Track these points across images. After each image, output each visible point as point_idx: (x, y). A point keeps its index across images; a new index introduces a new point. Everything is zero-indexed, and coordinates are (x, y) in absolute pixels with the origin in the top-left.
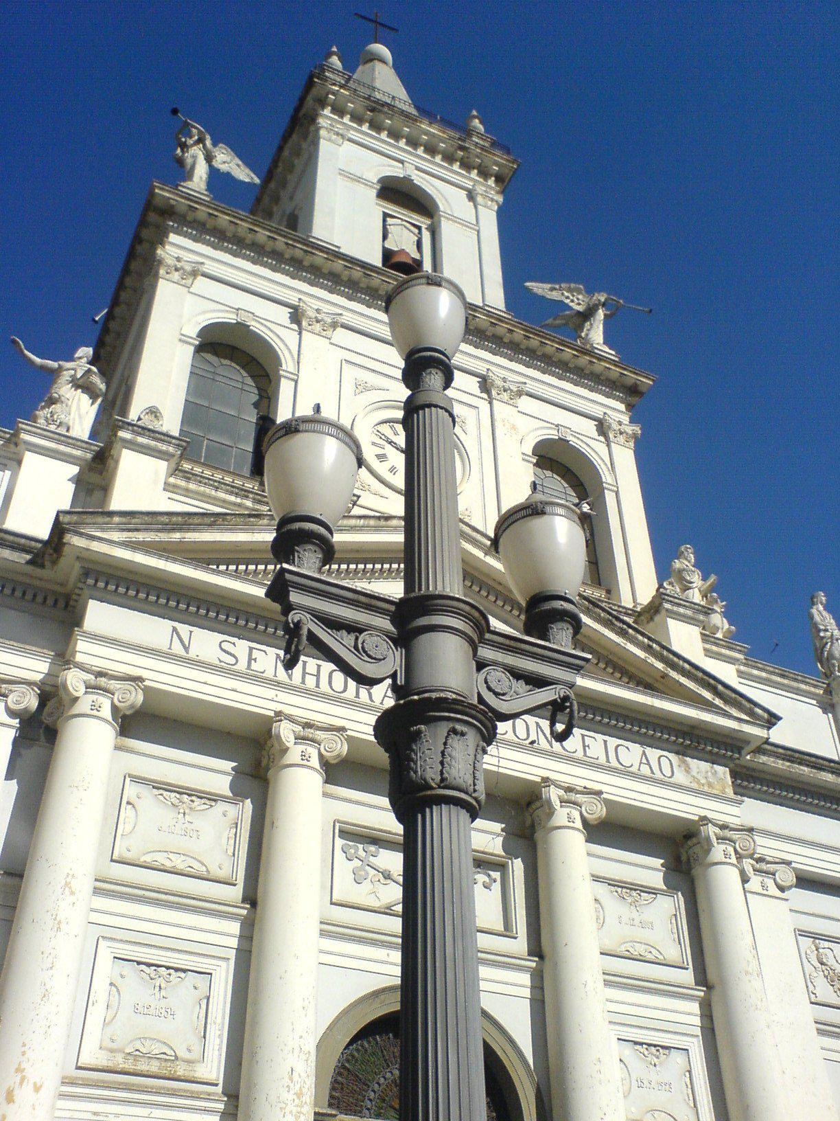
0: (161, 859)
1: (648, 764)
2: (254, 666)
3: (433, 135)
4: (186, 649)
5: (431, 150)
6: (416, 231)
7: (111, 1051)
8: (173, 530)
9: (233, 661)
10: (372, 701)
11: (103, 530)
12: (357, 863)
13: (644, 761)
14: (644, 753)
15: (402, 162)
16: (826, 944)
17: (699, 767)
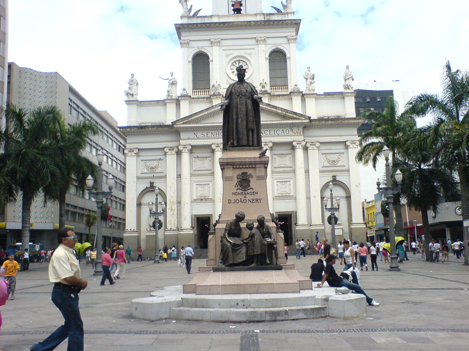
0: (200, 169)
4: (197, 136)
8: (189, 118)
11: (179, 122)
16: (328, 155)
17: (295, 130)
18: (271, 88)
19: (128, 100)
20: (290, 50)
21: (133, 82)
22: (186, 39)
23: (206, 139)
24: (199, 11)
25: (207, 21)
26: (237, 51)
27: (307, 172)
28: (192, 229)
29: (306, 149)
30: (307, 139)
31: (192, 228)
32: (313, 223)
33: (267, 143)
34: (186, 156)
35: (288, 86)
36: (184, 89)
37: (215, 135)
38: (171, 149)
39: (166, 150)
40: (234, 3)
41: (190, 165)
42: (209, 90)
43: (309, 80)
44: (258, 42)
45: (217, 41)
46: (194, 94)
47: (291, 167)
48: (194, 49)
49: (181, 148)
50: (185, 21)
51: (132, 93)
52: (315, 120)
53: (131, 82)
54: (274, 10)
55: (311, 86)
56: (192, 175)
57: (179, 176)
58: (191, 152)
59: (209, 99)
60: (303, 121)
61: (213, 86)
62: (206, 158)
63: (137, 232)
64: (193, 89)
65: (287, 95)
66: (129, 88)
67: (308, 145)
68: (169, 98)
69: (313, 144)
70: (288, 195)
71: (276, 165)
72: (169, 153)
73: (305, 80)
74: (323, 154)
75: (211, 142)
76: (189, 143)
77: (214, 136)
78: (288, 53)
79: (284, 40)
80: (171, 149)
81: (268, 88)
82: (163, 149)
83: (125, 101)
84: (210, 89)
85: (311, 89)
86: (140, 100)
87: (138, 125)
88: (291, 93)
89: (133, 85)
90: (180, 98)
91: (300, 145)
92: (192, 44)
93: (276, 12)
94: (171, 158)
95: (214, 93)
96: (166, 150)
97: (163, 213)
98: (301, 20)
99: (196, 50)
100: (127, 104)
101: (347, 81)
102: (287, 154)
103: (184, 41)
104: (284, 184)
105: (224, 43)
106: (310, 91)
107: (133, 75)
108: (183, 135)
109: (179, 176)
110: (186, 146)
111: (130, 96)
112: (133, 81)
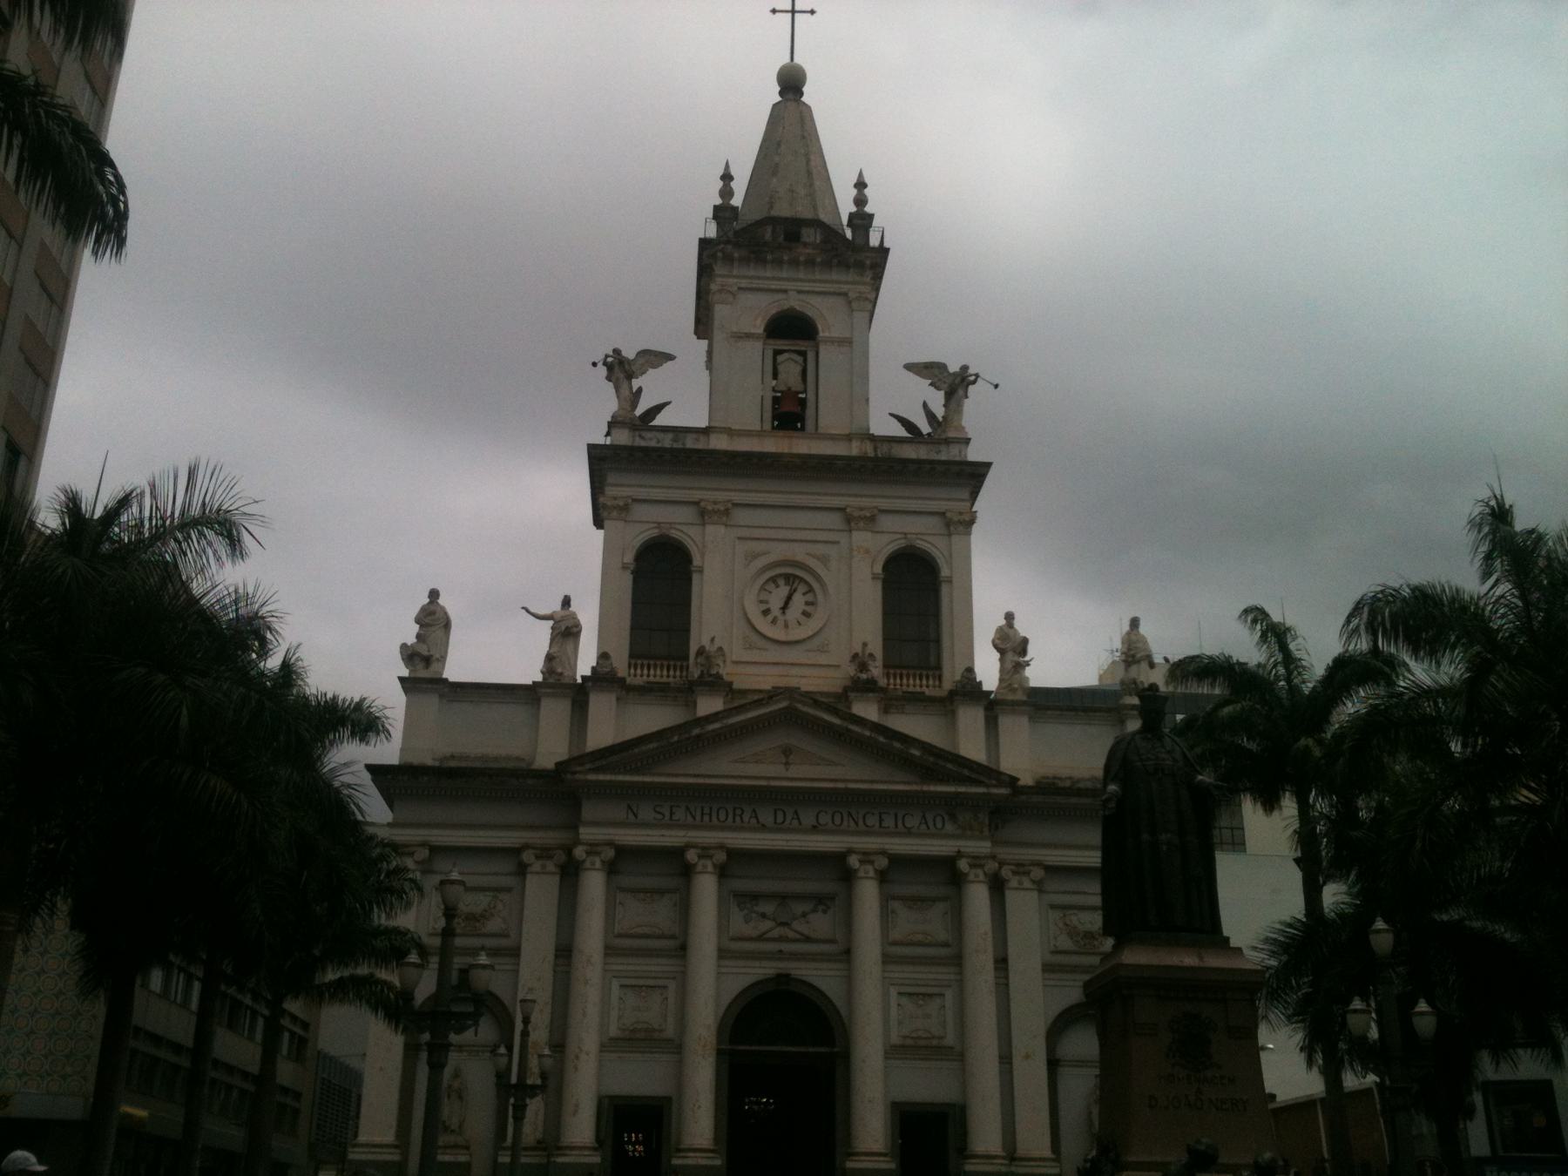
0: (640, 931)
1: (926, 823)
2: (674, 817)
3: (809, 254)
5: (810, 263)
6: (800, 359)
7: (624, 1030)
9: (660, 816)
10: (742, 822)
12: (746, 911)
13: (923, 821)
14: (924, 817)
15: (785, 291)
16: (1071, 912)
18: (886, 671)
19: (412, 675)
20: (951, 555)
21: (433, 620)
22: (625, 494)
23: (669, 827)
24: (658, 408)
25: (690, 443)
26: (785, 546)
27: (1002, 963)
28: (595, 1149)
29: (997, 887)
30: (1005, 853)
31: (597, 1145)
32: (1021, 1151)
33: (872, 858)
34: (594, 884)
35: (939, 667)
36: (603, 656)
37: (698, 818)
38: (544, 853)
39: (527, 856)
40: (779, 394)
41: (607, 914)
42: (685, 664)
43: (1010, 657)
44: (853, 524)
45: (722, 508)
46: (632, 671)
47: (946, 945)
48: (647, 526)
49: (579, 852)
50: (623, 437)
51: (425, 653)
52: (1026, 790)
53: (425, 617)
54: (899, 424)
55: (1017, 676)
56: (610, 951)
57: (565, 952)
58: (612, 869)
59: (687, 692)
60: (995, 791)
61: (701, 652)
62: (661, 892)
63: (396, 1147)
64: (631, 656)
65: (932, 700)
66: (418, 636)
67: (1006, 872)
68: (551, 680)
69: (1021, 869)
70: (935, 1042)
71: (896, 935)
72: (537, 866)
73: (997, 655)
74: (1053, 907)
75: (686, 840)
76: (607, 837)
77: (694, 818)
78: (945, 565)
79: (933, 523)
80: (544, 853)
81: (876, 670)
82: (515, 852)
83: (402, 679)
84: (686, 658)
85: (1016, 686)
86: (452, 679)
87: (437, 764)
88: (952, 694)
89: (433, 629)
90: (590, 684)
91: (980, 872)
92: (640, 511)
93: (901, 432)
94: (541, 890)
95: (702, 675)
96: (527, 856)
97: (543, 1088)
98: (988, 465)
99: (650, 532)
100: (406, 690)
101: (1134, 668)
102: (934, 900)
103: (615, 498)
104: (921, 1002)
105: (741, 516)
106: (1014, 690)
107: (434, 594)
108: (589, 811)
109: (565, 952)
110: (599, 849)
111: (420, 666)
112: (433, 613)
